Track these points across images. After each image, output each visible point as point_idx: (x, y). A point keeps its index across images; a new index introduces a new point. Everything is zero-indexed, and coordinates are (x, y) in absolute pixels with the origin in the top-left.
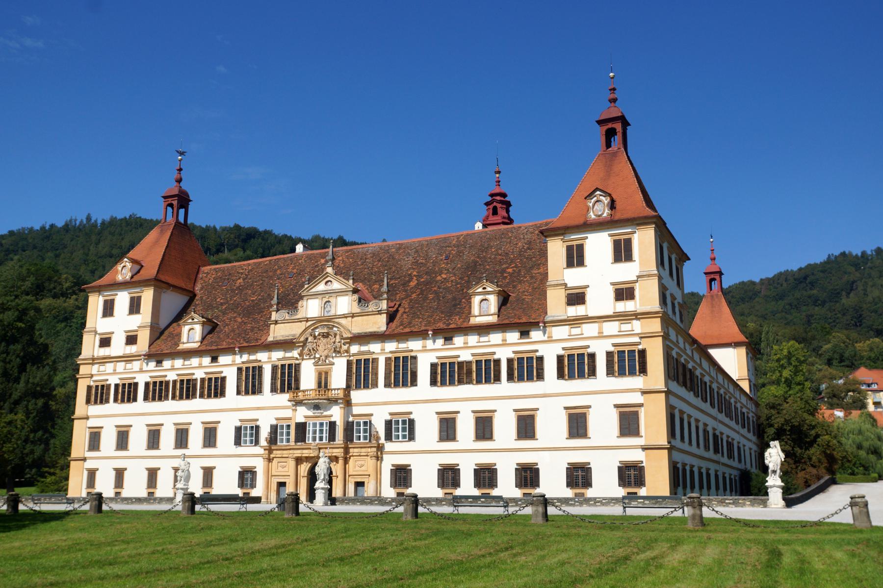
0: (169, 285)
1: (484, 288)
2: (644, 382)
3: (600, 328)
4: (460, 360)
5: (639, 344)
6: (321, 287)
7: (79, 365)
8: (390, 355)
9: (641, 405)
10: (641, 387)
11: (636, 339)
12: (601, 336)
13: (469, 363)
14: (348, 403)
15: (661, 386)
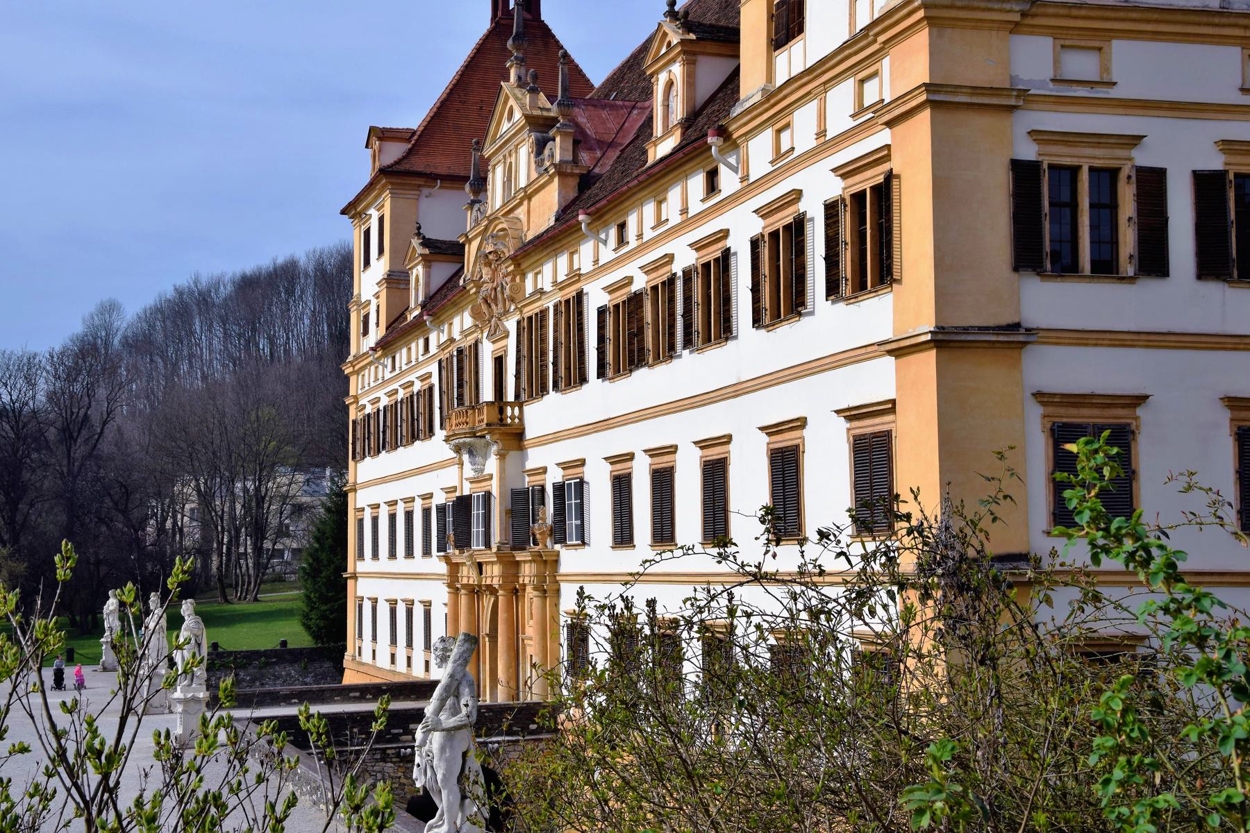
0: (431, 178)
1: (669, 43)
2: (898, 311)
3: (822, 116)
4: (635, 287)
5: (883, 156)
6: (505, 126)
7: (347, 378)
8: (559, 297)
9: (890, 407)
10: (888, 335)
11: (883, 137)
12: (826, 145)
13: (636, 299)
14: (515, 438)
15: (925, 324)
